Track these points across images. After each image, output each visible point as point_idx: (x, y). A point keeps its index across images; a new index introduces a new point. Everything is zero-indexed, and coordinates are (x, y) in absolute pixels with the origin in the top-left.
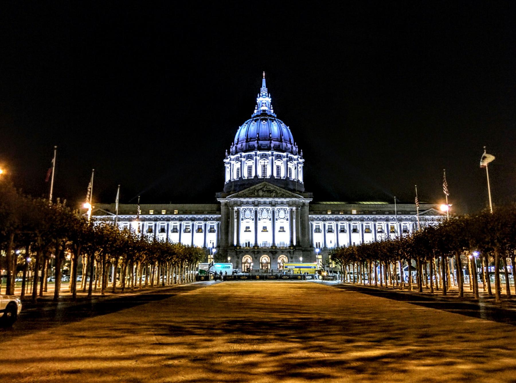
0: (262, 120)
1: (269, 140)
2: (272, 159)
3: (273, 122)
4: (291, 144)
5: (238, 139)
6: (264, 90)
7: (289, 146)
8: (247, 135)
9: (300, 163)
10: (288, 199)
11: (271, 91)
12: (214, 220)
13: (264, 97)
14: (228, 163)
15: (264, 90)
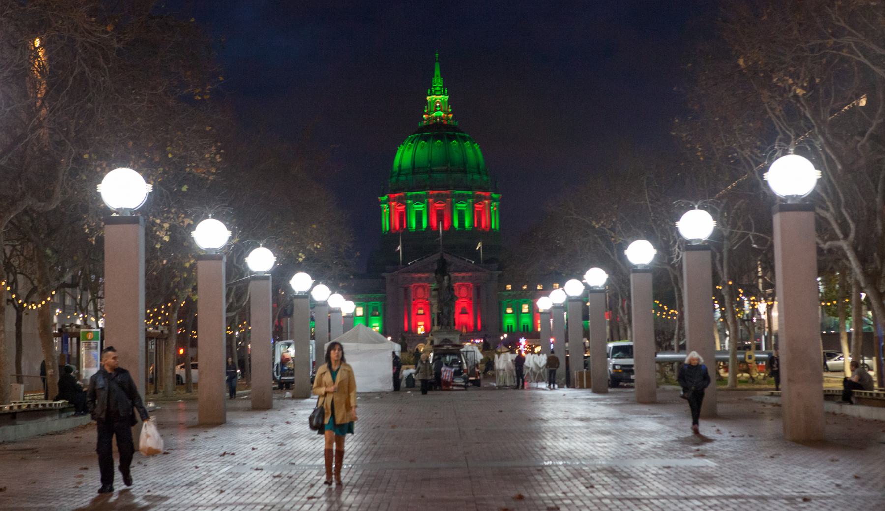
0: (436, 138)
1: (446, 171)
2: (452, 202)
3: (451, 140)
4: (480, 173)
5: (400, 166)
6: (438, 82)
7: (477, 177)
8: (413, 163)
9: (495, 200)
10: (470, 274)
11: (449, 85)
12: (377, 300)
13: (438, 93)
14: (385, 202)
15: (438, 82)
